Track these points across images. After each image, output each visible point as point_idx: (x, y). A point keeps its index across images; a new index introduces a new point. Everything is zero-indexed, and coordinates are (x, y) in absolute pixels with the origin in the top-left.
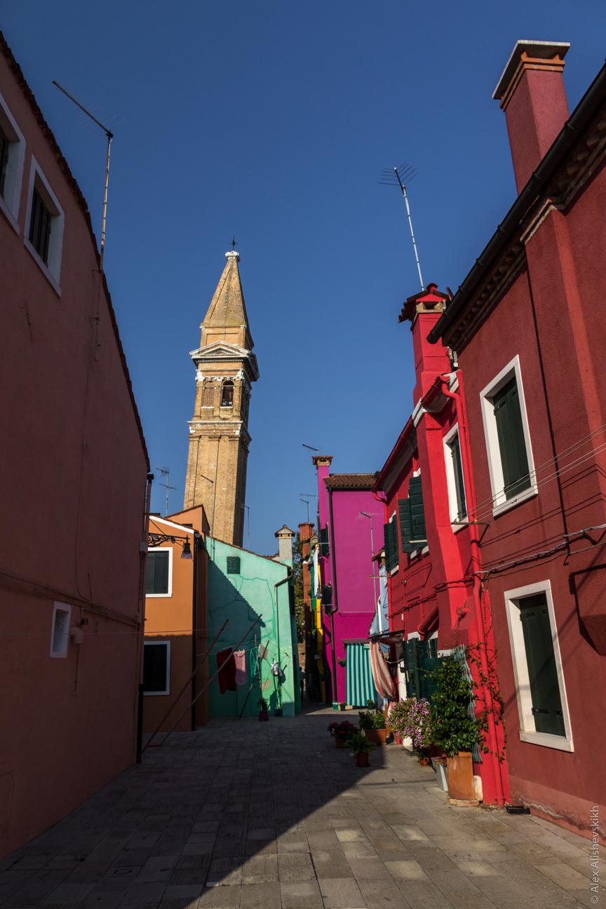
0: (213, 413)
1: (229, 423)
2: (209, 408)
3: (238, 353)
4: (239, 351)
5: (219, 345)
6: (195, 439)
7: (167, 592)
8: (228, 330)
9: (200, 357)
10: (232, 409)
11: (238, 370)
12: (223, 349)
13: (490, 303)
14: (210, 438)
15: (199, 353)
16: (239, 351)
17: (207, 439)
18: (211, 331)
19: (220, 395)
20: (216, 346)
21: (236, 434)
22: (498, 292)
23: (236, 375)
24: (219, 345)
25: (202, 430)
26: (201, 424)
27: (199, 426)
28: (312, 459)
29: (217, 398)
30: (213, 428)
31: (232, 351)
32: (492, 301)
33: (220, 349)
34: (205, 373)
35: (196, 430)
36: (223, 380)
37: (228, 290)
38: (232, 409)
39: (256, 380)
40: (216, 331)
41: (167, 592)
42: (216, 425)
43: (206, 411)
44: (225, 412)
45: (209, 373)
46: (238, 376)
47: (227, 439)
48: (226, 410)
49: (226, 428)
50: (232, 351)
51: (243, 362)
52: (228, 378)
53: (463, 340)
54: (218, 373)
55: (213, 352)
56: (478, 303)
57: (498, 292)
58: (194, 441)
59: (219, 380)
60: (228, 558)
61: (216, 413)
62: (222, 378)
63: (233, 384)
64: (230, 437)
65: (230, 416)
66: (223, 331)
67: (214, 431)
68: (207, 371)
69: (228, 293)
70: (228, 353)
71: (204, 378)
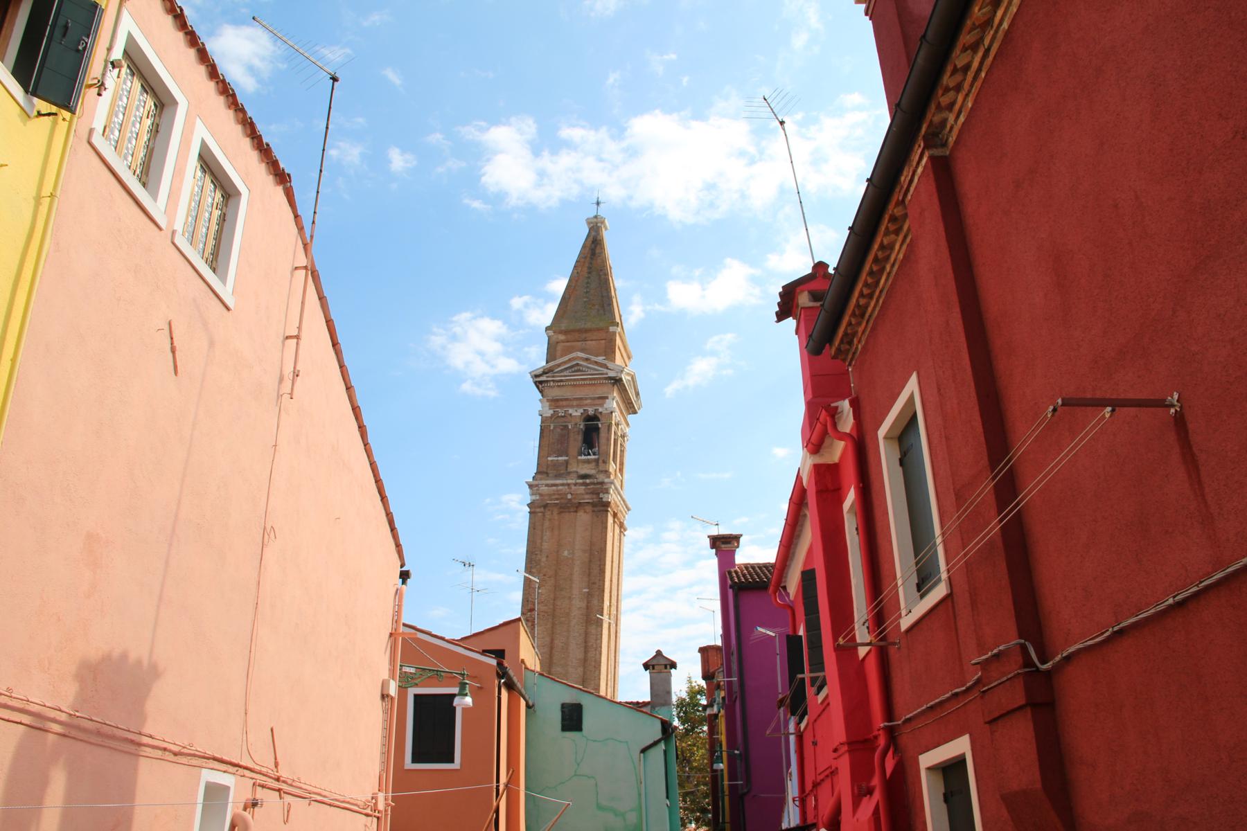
0: (567, 470)
1: (594, 484)
2: (560, 458)
3: (605, 371)
4: (607, 368)
7: (452, 760)
10: (597, 461)
12: (581, 365)
13: (881, 292)
16: (607, 368)
19: (580, 438)
20: (570, 360)
22: (889, 274)
23: (602, 405)
26: (547, 485)
28: (708, 539)
29: (576, 441)
31: (596, 367)
32: (883, 287)
33: (577, 364)
34: (553, 404)
37: (589, 273)
39: (635, 412)
41: (452, 760)
42: (573, 487)
43: (555, 465)
44: (586, 465)
48: (588, 462)
50: (596, 367)
52: (591, 412)
53: (857, 348)
54: (575, 403)
55: (566, 369)
56: (866, 291)
57: (889, 274)
59: (577, 413)
60: (563, 706)
61: (573, 468)
62: (582, 411)
65: (593, 472)
67: (569, 496)
68: (557, 400)
69: (589, 278)
71: (551, 412)
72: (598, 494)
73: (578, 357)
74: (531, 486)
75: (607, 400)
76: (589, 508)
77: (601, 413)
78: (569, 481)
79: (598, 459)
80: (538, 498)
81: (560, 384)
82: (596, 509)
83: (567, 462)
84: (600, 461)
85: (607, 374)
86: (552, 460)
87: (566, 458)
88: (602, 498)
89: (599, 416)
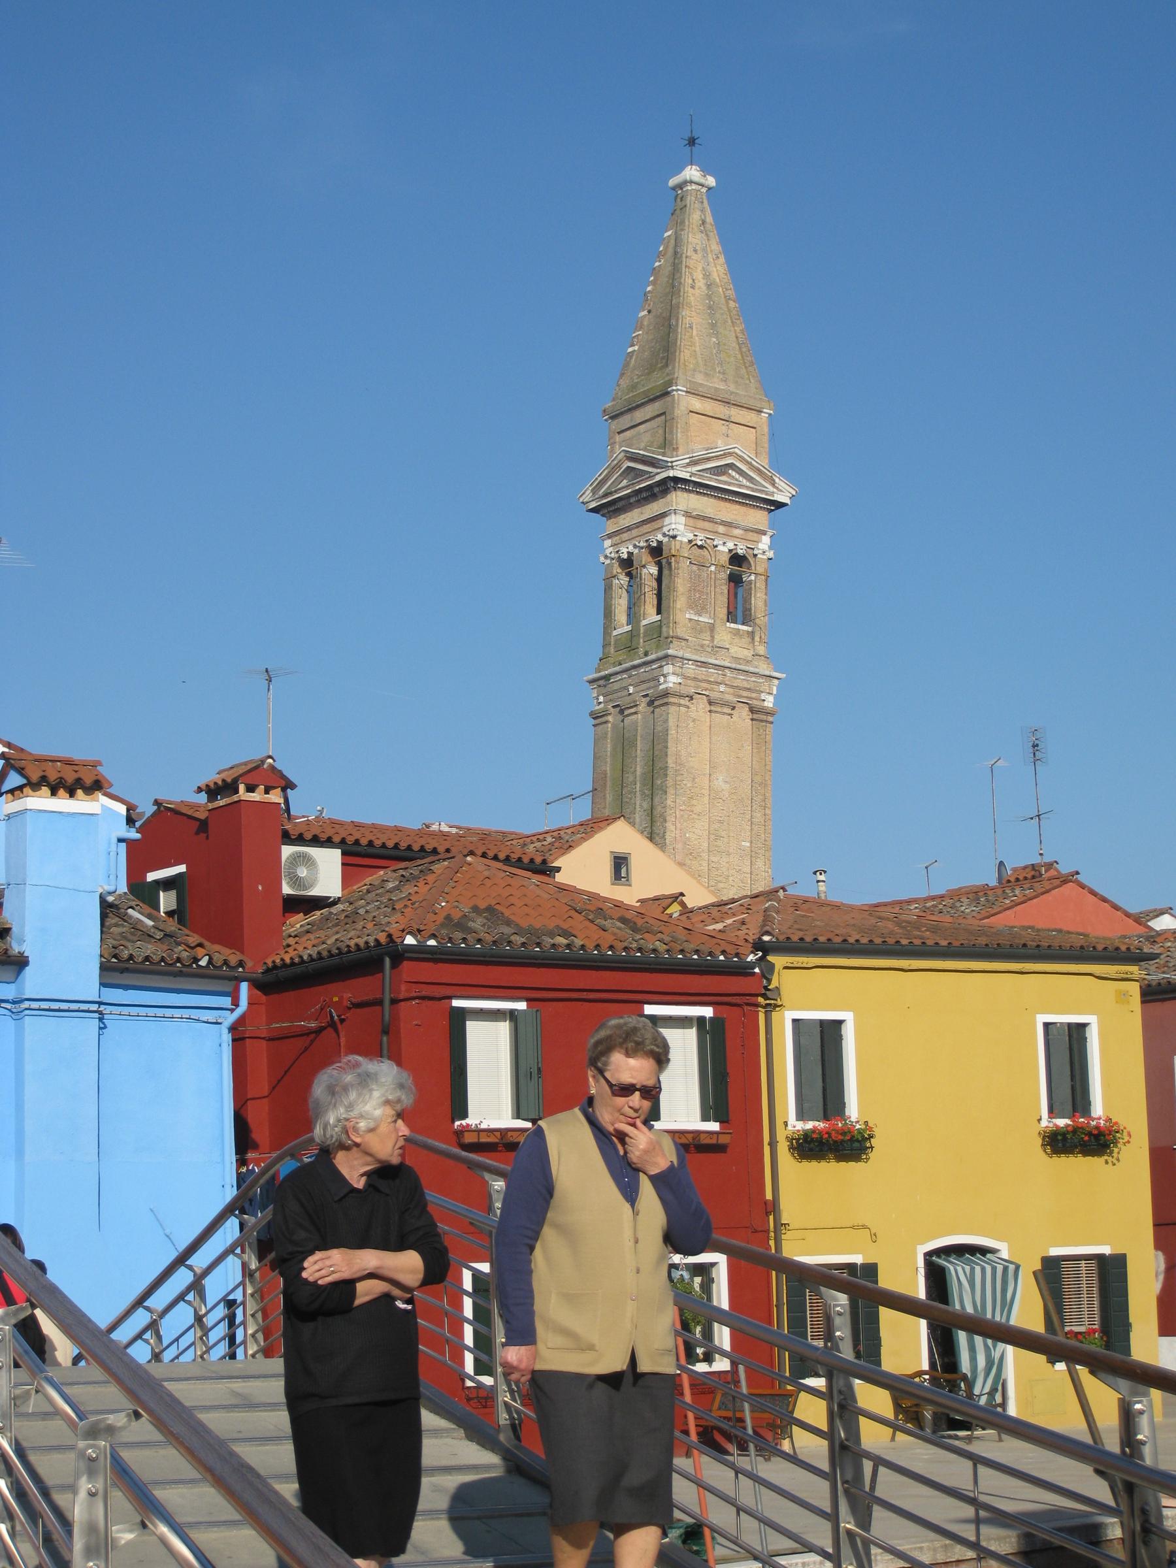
3: (771, 489)
4: (773, 484)
5: (730, 454)
6: (682, 702)
9: (686, 476)
11: (764, 533)
14: (710, 703)
15: (688, 465)
16: (773, 484)
17: (701, 704)
18: (697, 404)
21: (766, 704)
24: (730, 454)
25: (695, 679)
27: (690, 670)
30: (720, 679)
31: (758, 478)
34: (691, 522)
35: (685, 677)
38: (752, 635)
45: (701, 524)
46: (761, 546)
47: (745, 711)
48: (737, 633)
49: (746, 685)
50: (758, 478)
54: (721, 529)
58: (680, 705)
59: (725, 548)
64: (752, 710)
69: (709, 297)
70: (745, 482)
73: (736, 454)
75: (763, 537)
77: (755, 556)
79: (753, 632)
80: (679, 681)
82: (755, 716)
85: (772, 494)
86: (690, 620)
87: (711, 621)
88: (764, 700)
89: (751, 560)
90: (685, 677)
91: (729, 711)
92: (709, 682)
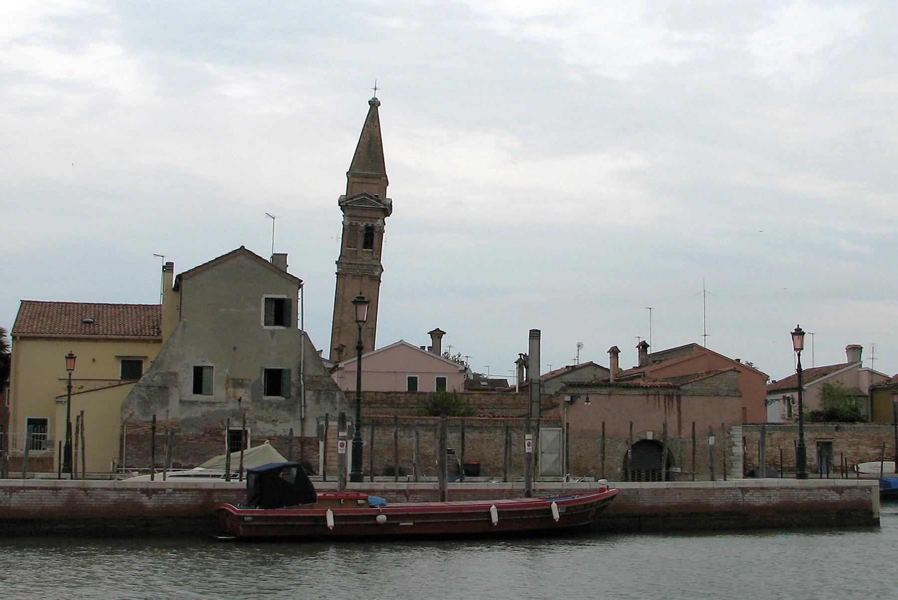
8: (369, 180)
10: (372, 252)
17: (350, 276)
19: (363, 239)
23: (376, 222)
26: (347, 263)
29: (361, 240)
36: (365, 226)
38: (372, 252)
40: (360, 180)
45: (354, 218)
46: (378, 223)
51: (383, 211)
59: (362, 225)
61: (360, 254)
62: (365, 224)
63: (373, 230)
66: (364, 180)
72: (373, 271)
74: (337, 262)
76: (367, 278)
78: (358, 263)
81: (353, 208)
82: (371, 278)
83: (356, 251)
84: (374, 253)
90: (343, 268)
91: (360, 278)
92: (351, 269)
